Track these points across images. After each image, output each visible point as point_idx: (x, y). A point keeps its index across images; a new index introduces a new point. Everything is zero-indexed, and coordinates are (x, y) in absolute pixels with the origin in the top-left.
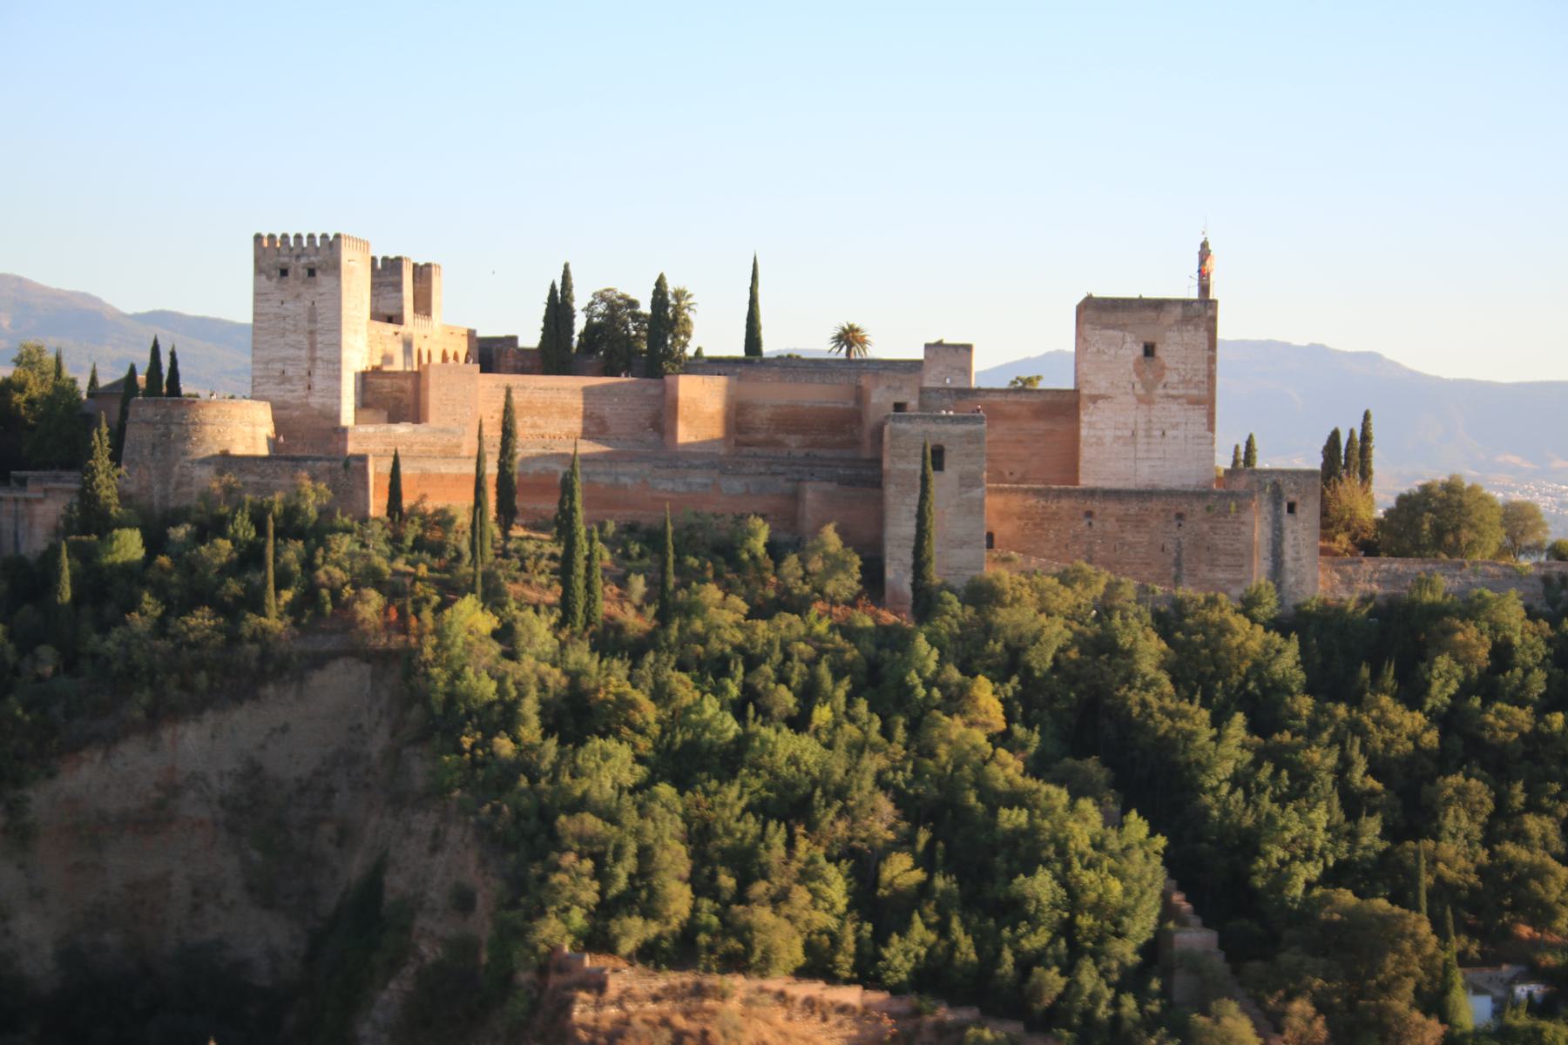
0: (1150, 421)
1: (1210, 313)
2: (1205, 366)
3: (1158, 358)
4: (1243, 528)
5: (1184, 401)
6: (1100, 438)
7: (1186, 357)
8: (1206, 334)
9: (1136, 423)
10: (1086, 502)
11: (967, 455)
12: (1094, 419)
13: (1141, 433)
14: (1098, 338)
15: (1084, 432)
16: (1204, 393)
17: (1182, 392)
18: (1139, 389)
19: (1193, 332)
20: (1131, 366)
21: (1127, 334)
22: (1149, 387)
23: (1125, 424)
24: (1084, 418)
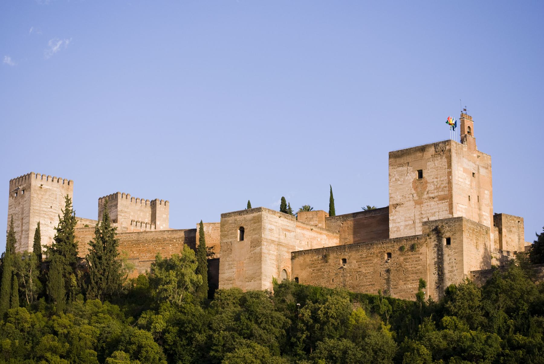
0: (422, 214)
1: (447, 147)
2: (446, 178)
3: (424, 177)
4: (421, 257)
5: (437, 199)
6: (398, 228)
7: (437, 174)
8: (446, 160)
9: (415, 216)
10: (341, 254)
11: (254, 230)
12: (395, 217)
13: (417, 221)
14: (395, 173)
15: (391, 226)
16: (446, 193)
17: (436, 194)
18: (416, 198)
19: (440, 160)
20: (411, 185)
21: (408, 168)
22: (420, 195)
23: (409, 217)
24: (391, 218)
